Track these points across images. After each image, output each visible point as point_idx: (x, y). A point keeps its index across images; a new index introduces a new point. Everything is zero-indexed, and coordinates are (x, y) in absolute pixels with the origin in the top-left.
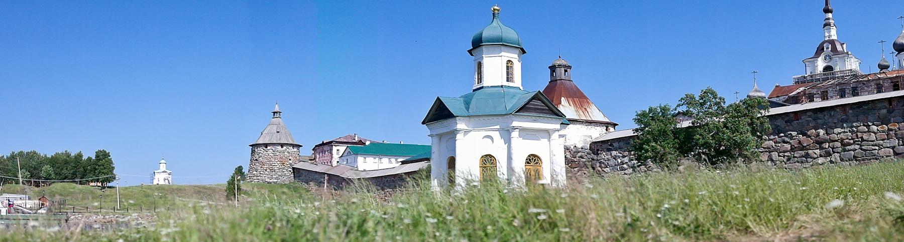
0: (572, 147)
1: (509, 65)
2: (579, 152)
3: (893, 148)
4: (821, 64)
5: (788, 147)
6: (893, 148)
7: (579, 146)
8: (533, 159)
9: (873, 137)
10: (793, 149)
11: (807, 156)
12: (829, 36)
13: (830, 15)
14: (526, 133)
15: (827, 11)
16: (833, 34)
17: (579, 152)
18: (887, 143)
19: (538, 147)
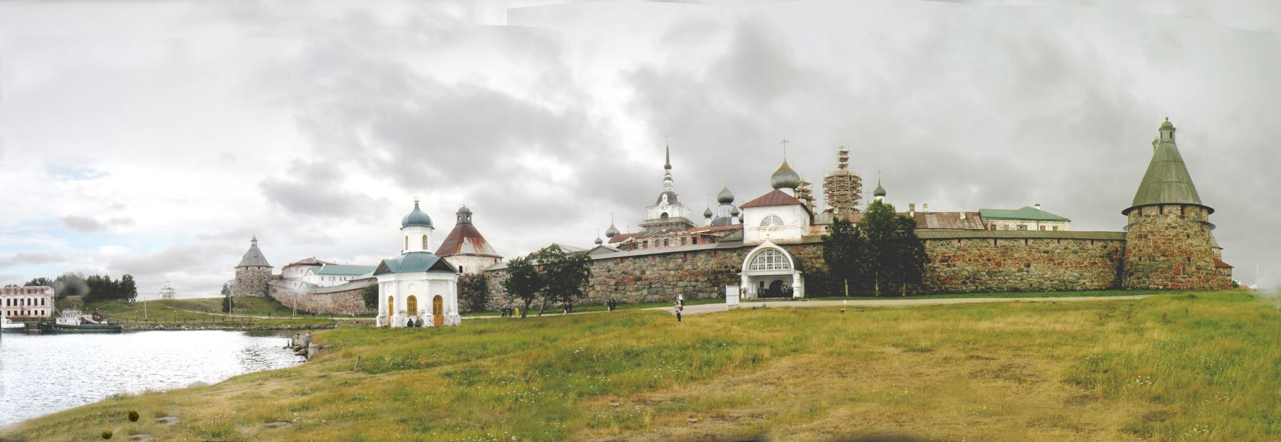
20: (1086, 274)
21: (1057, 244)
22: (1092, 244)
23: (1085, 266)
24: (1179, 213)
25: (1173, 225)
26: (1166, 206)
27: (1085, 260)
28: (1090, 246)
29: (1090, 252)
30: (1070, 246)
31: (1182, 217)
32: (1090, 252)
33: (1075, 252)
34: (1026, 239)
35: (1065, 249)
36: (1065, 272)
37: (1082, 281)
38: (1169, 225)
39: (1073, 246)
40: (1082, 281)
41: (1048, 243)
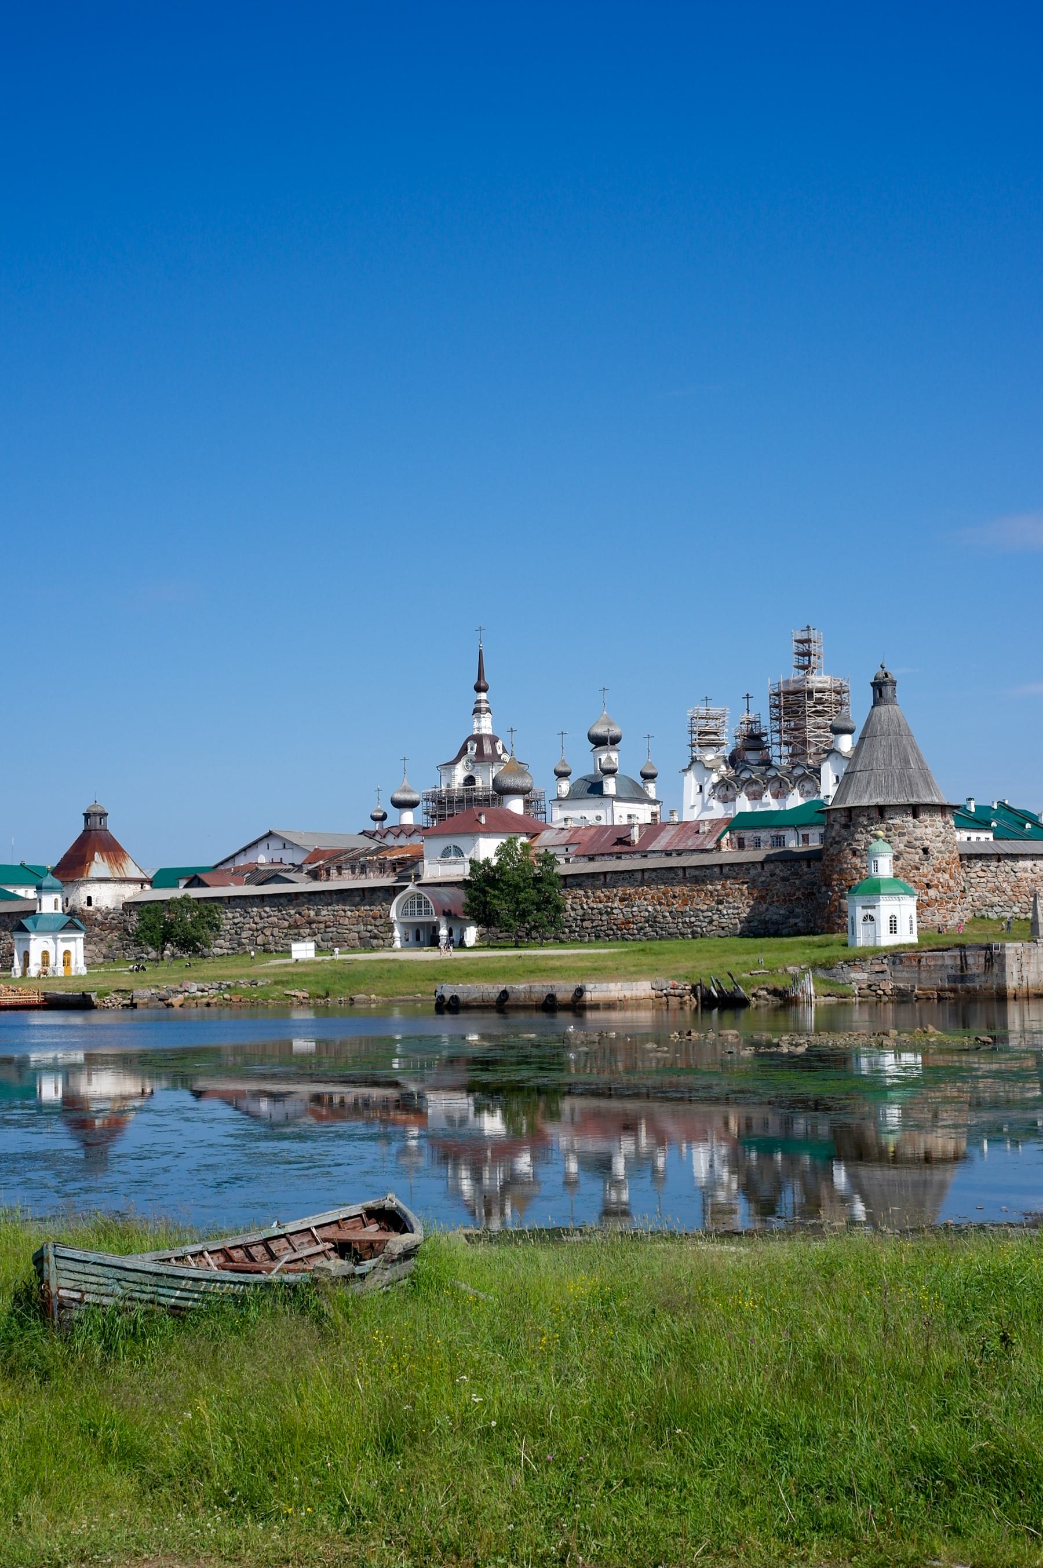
0: (104, 908)
1: (56, 901)
2: (111, 913)
3: (358, 933)
4: (460, 773)
5: (286, 924)
6: (358, 933)
7: (111, 907)
8: (67, 953)
9: (347, 921)
10: (290, 927)
11: (299, 934)
12: (479, 729)
13: (483, 696)
14: (64, 940)
15: (479, 689)
16: (485, 725)
17: (111, 913)
18: (355, 928)
19: (69, 946)
20: (797, 910)
21: (759, 870)
22: (809, 866)
23: (798, 899)
24: (843, 820)
25: (837, 839)
26: (888, 808)
27: (798, 889)
28: (806, 870)
29: (805, 878)
30: (777, 871)
31: (846, 826)
32: (805, 878)
33: (785, 879)
34: (721, 866)
35: (772, 875)
36: (767, 909)
37: (792, 921)
38: (834, 838)
39: (781, 871)
40: (792, 921)
41: (748, 869)
